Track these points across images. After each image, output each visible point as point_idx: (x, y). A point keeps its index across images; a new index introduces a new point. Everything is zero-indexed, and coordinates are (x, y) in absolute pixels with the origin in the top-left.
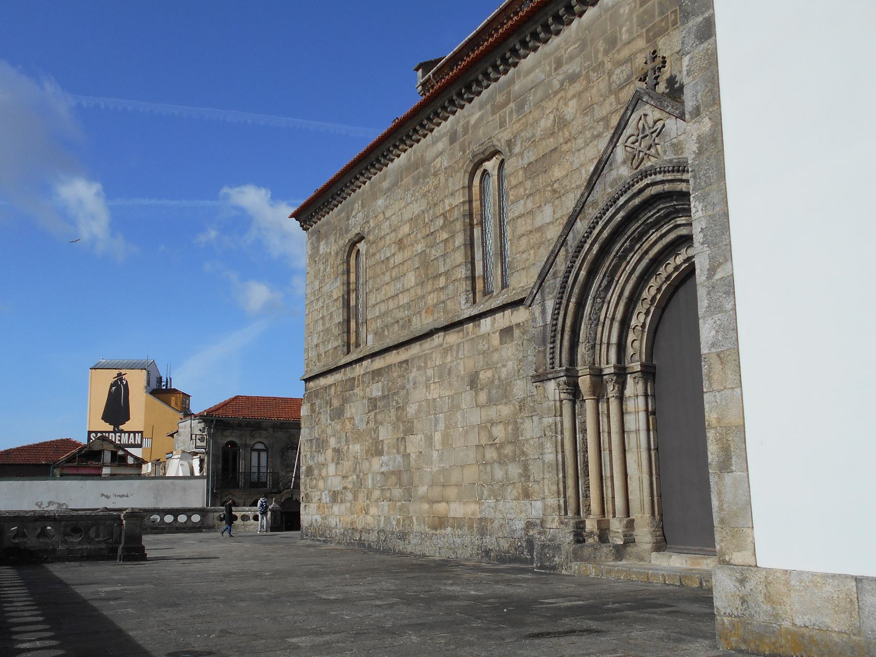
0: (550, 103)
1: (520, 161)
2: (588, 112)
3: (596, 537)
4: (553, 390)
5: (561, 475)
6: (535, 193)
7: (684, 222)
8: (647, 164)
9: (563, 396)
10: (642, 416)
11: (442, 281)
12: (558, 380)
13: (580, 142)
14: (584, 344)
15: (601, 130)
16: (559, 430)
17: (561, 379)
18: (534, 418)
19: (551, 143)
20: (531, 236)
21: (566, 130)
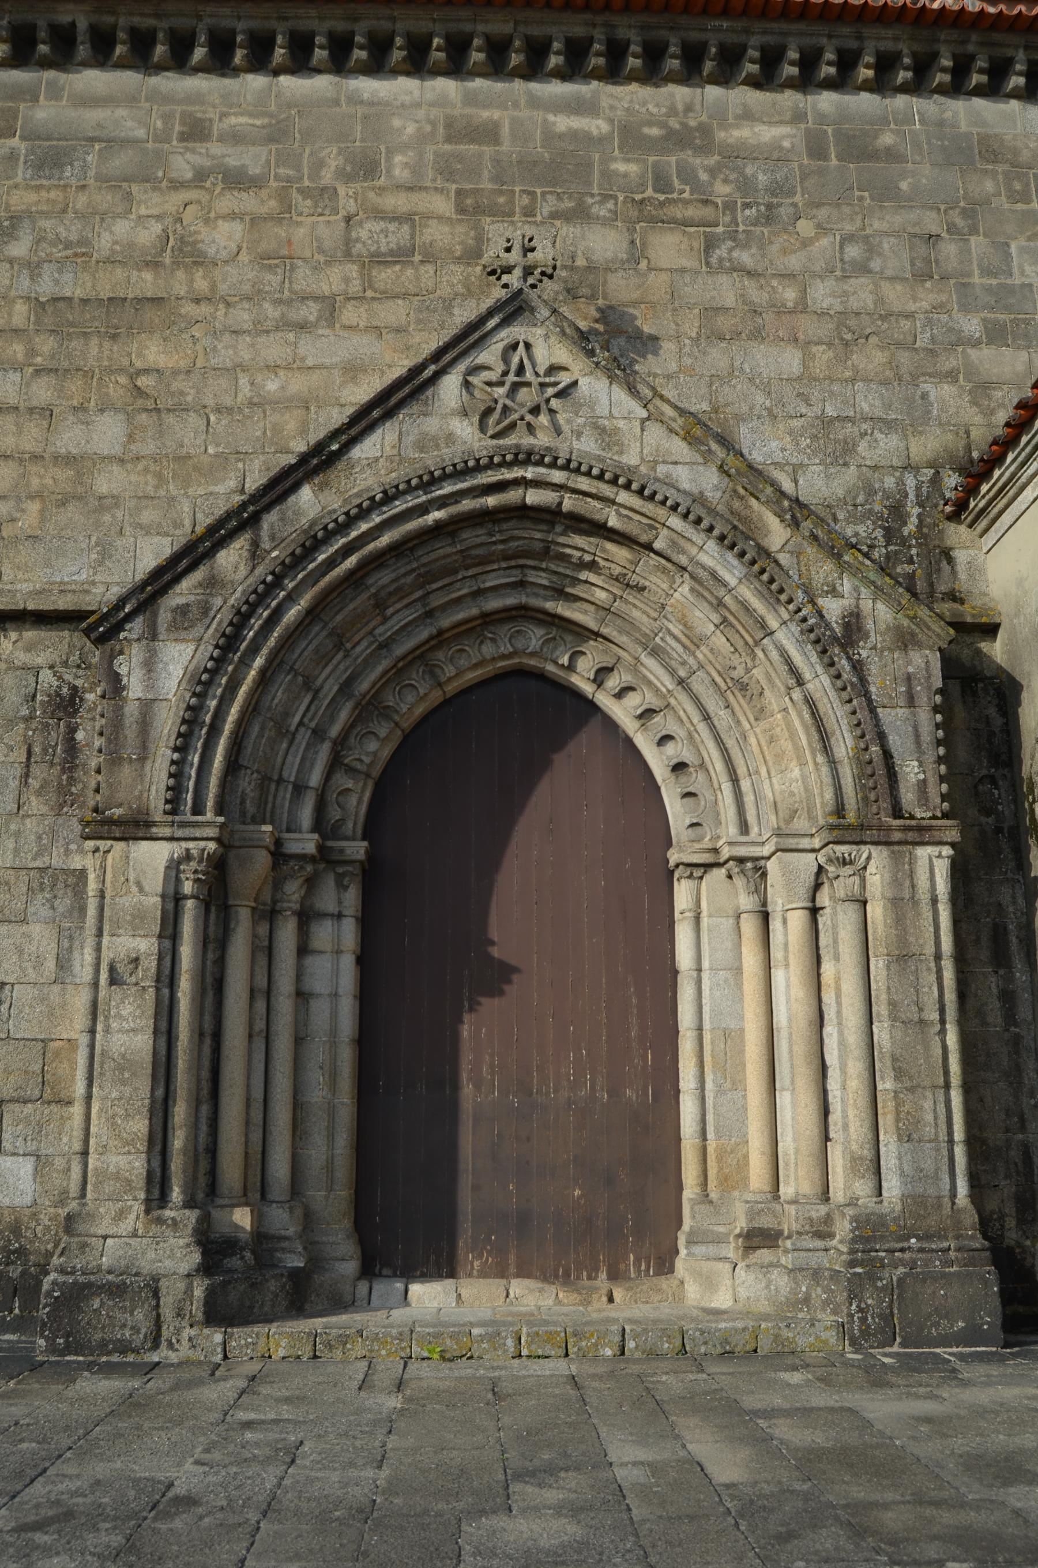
0: (156, 198)
1: (27, 283)
2: (277, 266)
3: (248, 1255)
6: (67, 371)
7: (545, 582)
8: (519, 439)
10: (348, 963)
13: (242, 316)
14: (249, 772)
19: (147, 283)
20: (33, 468)
21: (200, 274)
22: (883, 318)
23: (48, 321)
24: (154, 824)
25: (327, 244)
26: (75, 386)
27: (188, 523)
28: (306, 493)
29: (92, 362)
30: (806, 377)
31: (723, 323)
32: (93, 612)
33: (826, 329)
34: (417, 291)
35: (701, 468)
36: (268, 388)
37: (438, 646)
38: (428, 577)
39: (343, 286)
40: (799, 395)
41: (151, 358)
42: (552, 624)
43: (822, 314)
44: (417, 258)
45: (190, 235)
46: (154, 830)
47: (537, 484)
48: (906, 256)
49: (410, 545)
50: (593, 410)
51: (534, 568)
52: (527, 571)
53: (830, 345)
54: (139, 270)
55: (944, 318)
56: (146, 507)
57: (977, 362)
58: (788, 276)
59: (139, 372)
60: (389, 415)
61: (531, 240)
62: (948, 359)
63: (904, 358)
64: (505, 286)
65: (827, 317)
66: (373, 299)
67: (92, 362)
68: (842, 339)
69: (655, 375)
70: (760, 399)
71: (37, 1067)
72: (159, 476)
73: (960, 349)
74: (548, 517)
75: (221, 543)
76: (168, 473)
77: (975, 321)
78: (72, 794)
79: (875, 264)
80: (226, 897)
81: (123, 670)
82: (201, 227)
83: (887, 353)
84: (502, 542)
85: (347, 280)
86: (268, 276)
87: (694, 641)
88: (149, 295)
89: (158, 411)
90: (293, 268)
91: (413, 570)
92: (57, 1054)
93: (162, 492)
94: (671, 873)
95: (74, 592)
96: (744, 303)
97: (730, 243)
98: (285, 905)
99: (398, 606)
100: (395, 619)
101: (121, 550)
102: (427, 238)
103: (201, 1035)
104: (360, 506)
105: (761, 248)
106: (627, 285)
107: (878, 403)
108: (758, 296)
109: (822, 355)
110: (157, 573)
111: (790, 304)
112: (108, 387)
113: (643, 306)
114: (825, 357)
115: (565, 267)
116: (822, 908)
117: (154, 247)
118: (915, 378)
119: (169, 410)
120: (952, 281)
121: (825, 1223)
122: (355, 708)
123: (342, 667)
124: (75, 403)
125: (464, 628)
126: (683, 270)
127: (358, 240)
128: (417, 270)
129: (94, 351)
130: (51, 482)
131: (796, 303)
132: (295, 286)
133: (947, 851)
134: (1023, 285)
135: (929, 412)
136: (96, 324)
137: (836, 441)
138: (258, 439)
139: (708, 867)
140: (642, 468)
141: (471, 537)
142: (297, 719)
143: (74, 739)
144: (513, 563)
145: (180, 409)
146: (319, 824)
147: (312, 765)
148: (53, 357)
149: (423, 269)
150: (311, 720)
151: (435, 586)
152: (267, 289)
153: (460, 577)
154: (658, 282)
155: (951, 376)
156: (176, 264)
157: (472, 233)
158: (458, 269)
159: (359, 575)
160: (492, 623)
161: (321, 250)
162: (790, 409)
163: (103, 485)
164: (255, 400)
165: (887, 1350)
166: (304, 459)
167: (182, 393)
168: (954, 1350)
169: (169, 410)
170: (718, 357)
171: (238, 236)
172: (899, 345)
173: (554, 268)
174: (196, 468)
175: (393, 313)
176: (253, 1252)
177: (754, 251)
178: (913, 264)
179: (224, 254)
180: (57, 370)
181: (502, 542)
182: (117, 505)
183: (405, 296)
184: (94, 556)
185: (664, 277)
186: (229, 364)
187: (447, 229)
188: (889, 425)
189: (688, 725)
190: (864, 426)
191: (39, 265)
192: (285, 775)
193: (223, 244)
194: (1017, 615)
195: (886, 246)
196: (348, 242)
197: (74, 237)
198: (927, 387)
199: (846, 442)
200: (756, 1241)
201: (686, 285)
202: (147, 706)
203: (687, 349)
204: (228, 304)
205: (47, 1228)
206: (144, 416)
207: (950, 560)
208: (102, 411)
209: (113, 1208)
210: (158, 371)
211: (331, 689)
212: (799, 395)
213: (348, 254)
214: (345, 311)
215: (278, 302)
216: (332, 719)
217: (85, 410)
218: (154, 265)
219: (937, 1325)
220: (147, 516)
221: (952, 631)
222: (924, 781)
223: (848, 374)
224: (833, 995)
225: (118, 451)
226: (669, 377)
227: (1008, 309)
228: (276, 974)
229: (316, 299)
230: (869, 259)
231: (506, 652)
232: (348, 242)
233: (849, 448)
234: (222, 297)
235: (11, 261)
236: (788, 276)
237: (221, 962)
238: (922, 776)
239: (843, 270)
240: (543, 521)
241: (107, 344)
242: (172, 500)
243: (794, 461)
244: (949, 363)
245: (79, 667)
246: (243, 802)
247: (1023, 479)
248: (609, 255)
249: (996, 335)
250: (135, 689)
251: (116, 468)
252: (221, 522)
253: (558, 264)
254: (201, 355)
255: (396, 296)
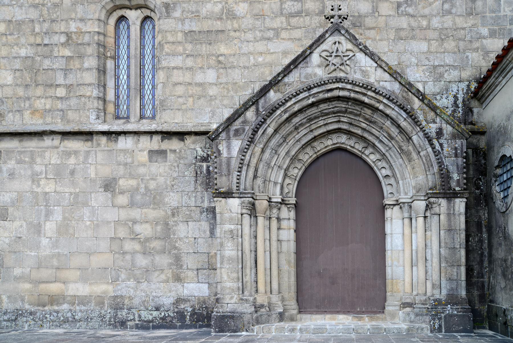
1: (180, 26)
2: (259, 18)
3: (267, 308)
4: (237, 206)
5: (240, 266)
6: (196, 56)
7: (346, 121)
9: (244, 211)
11: (61, 92)
12: (242, 199)
13: (250, 36)
15: (272, 36)
16: (240, 234)
17: (248, 199)
18: (190, 223)
19: (218, 25)
20: (189, 87)
21: (235, 22)
22: (455, 30)
23: (189, 39)
24: (233, 193)
25: (275, 10)
26: (199, 60)
27: (238, 104)
28: (272, 93)
29: (204, 52)
30: (429, 52)
31: (403, 34)
32: (210, 132)
33: (435, 35)
34: (304, 26)
35: (394, 83)
36: (259, 60)
37: (315, 141)
38: (310, 120)
39: (281, 25)
40: (426, 58)
41: (222, 51)
42: (349, 134)
43: (435, 29)
44: (304, 14)
45: (231, 8)
46: (234, 195)
47: (343, 89)
48: (464, 7)
49: (304, 109)
50: (360, 64)
51: (343, 116)
52: (340, 117)
53: (437, 40)
54: (216, 21)
55: (476, 29)
56: (225, 99)
57: (485, 44)
58: (424, 16)
59: (218, 56)
60: (296, 67)
61: (340, 6)
62: (476, 44)
63: (461, 44)
64: (332, 23)
65: (436, 31)
66: (291, 29)
67: (204, 52)
68: (441, 38)
69: (381, 53)
70: (414, 60)
71: (207, 260)
72: (228, 89)
73: (480, 40)
74: (346, 100)
75: (246, 109)
76: (230, 88)
77: (486, 29)
78: (210, 185)
79: (454, 11)
80: (256, 214)
81: (221, 149)
82: (234, 5)
83: (456, 42)
84: (333, 108)
85: (282, 23)
86: (257, 22)
87: (391, 138)
88: (220, 29)
89: (226, 68)
90: (264, 19)
91: (306, 117)
92: (212, 256)
93: (229, 95)
94: (384, 208)
95: (205, 126)
96: (409, 27)
97: (406, 5)
98: (273, 216)
99: (302, 129)
100: (301, 133)
101: (218, 113)
102: (307, 7)
103: (251, 251)
104: (288, 97)
105: (415, 7)
106: (372, 22)
107: (452, 60)
108: (414, 24)
109: (434, 44)
110: (228, 119)
111: (424, 26)
112: (209, 60)
113: (376, 29)
114: (435, 45)
115: (351, 16)
116: (427, 217)
117: (220, 12)
118: (464, 51)
119: (229, 68)
120: (480, 15)
121: (425, 301)
122: (291, 160)
123: (286, 147)
124: (200, 66)
125: (322, 135)
126: (390, 16)
127: (285, 8)
128: (304, 19)
129: (204, 49)
130: (195, 91)
131: (427, 26)
132: (265, 25)
133: (465, 200)
134: (504, 15)
135: (468, 63)
136: (204, 40)
137: (438, 73)
138: (257, 77)
139: (394, 205)
140: (375, 83)
141: (323, 106)
142: (274, 163)
143: (209, 170)
144: (336, 115)
145: (233, 67)
146: (281, 193)
147: (279, 176)
148: (191, 51)
149: (306, 18)
150: (278, 163)
151: (313, 123)
152: (257, 26)
153: (320, 119)
154: (382, 20)
155: (476, 50)
156: (227, 18)
157: (321, 5)
158: (317, 18)
159: (289, 119)
160: (331, 134)
161: (273, 13)
162: (423, 63)
163: (211, 93)
164: (256, 64)
165: (440, 334)
166: (270, 82)
167: (233, 62)
168: (459, 334)
169: (229, 68)
170: (401, 46)
171: (246, 8)
172: (460, 39)
173: (348, 16)
174: (239, 87)
175: (297, 34)
176: (269, 307)
177: (413, 7)
178: (466, 10)
179: (242, 15)
180: (193, 55)
181: (333, 108)
182: (216, 99)
183: (300, 28)
184: (210, 115)
185: (384, 18)
186: (246, 52)
187: (313, 4)
188: (455, 67)
189: (389, 164)
190: (447, 68)
191: (184, 20)
192: (271, 180)
193: (242, 11)
194: (491, 128)
195: (458, 4)
196: (281, 9)
197: (194, 10)
198: (468, 54)
199: (441, 74)
200: (406, 306)
201: (391, 21)
202: (229, 159)
203: (390, 44)
204: (245, 32)
205: (213, 302)
206: (222, 70)
207: (472, 112)
208: (208, 68)
209: (229, 296)
210: (224, 55)
211: (283, 154)
212: (426, 58)
213: (282, 13)
214: (282, 34)
215: (261, 31)
216: (284, 163)
217: (203, 68)
218: (220, 19)
219: (455, 328)
220: (226, 102)
221: (470, 133)
222: (459, 179)
223: (442, 50)
224: (429, 240)
225: (214, 81)
226: (385, 53)
227: (498, 25)
228: (272, 235)
229: (272, 29)
230: (451, 9)
231: (335, 143)
232: (281, 9)
233: (441, 75)
234: (243, 30)
235: (175, 18)
236: (424, 16)
237: (256, 231)
238: (458, 178)
239: (443, 13)
240: (345, 101)
241: (208, 46)
242: (232, 97)
243: (424, 80)
244: (476, 45)
245: (209, 148)
246: (259, 187)
247: (497, 83)
248: (366, 11)
249: (493, 34)
250: (225, 154)
251: (214, 87)
252: (246, 103)
253: (349, 15)
254: (238, 49)
255: (297, 28)
